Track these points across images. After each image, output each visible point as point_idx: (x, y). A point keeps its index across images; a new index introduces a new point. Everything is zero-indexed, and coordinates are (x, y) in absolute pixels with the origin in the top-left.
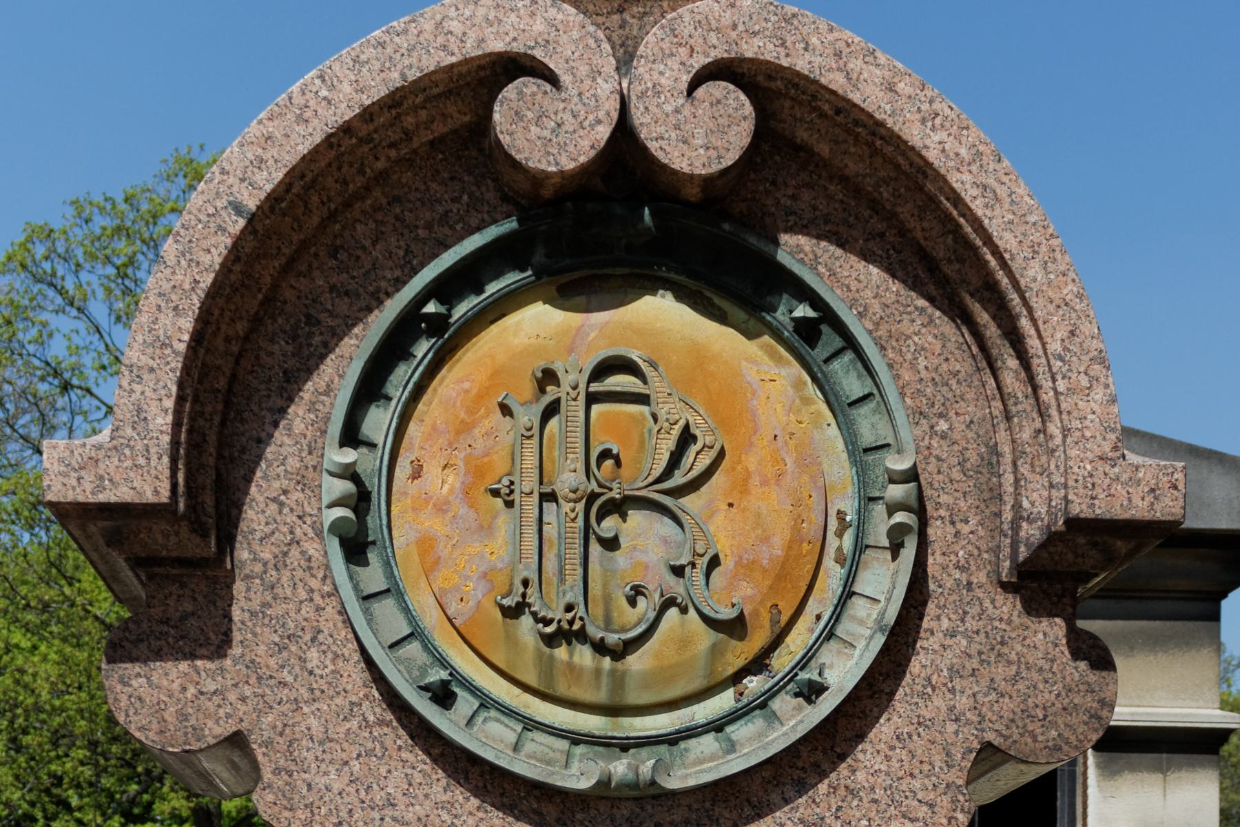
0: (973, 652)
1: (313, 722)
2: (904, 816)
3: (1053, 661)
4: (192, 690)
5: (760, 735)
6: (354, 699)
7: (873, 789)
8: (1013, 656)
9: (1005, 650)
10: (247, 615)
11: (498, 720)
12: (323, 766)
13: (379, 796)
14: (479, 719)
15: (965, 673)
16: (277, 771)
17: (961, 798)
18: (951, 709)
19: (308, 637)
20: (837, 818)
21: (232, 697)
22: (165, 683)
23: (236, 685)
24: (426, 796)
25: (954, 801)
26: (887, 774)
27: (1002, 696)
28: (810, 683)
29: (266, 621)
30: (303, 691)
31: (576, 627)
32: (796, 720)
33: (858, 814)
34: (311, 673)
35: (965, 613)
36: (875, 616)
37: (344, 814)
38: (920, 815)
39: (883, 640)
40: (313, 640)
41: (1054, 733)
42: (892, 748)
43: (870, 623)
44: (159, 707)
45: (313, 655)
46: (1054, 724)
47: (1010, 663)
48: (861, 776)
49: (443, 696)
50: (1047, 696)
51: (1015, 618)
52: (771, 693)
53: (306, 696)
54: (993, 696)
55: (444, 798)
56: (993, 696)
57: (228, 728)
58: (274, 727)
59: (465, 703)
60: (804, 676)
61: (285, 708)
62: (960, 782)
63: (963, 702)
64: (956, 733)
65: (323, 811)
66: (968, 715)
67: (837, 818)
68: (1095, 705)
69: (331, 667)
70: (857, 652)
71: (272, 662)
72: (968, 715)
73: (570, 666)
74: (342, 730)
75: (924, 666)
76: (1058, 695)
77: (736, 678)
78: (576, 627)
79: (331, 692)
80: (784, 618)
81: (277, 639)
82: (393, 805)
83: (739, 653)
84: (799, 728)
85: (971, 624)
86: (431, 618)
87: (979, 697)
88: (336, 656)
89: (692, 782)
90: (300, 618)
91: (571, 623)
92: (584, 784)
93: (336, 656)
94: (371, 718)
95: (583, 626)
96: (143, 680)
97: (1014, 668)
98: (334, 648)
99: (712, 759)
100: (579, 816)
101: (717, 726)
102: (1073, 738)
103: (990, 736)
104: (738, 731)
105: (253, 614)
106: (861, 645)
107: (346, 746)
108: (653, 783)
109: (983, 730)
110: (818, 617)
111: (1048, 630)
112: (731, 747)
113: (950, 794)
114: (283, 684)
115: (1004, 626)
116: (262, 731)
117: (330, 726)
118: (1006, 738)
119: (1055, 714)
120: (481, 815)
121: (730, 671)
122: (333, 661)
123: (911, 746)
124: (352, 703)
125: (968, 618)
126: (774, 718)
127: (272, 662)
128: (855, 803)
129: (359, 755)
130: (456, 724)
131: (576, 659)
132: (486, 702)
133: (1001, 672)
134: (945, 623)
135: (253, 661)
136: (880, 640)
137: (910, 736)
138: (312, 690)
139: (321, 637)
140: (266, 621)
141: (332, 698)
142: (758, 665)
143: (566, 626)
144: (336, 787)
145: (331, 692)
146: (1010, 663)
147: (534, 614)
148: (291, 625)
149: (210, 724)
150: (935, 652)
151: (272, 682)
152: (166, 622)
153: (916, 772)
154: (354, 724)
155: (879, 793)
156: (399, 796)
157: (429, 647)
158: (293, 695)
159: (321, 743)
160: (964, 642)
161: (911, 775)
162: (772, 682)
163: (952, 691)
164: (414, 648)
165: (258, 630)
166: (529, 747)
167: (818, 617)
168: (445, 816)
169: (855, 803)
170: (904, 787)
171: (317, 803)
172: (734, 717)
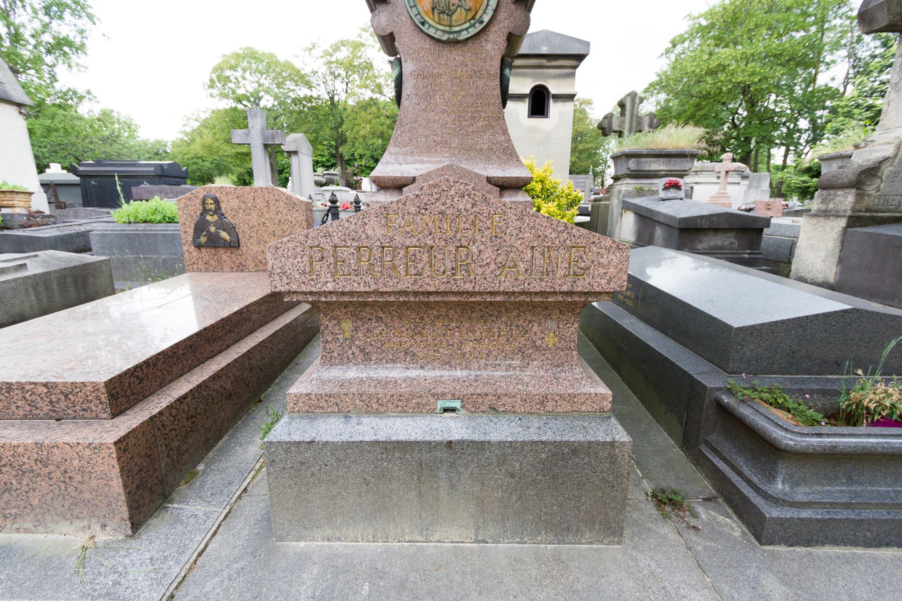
32: (479, 27)
49: (423, 24)
59: (427, 26)
83: (470, 16)
86: (421, 11)
101: (467, 29)
104: (470, 30)
132: (430, 26)
133: (512, 19)
142: (473, 18)
172: (469, 27)
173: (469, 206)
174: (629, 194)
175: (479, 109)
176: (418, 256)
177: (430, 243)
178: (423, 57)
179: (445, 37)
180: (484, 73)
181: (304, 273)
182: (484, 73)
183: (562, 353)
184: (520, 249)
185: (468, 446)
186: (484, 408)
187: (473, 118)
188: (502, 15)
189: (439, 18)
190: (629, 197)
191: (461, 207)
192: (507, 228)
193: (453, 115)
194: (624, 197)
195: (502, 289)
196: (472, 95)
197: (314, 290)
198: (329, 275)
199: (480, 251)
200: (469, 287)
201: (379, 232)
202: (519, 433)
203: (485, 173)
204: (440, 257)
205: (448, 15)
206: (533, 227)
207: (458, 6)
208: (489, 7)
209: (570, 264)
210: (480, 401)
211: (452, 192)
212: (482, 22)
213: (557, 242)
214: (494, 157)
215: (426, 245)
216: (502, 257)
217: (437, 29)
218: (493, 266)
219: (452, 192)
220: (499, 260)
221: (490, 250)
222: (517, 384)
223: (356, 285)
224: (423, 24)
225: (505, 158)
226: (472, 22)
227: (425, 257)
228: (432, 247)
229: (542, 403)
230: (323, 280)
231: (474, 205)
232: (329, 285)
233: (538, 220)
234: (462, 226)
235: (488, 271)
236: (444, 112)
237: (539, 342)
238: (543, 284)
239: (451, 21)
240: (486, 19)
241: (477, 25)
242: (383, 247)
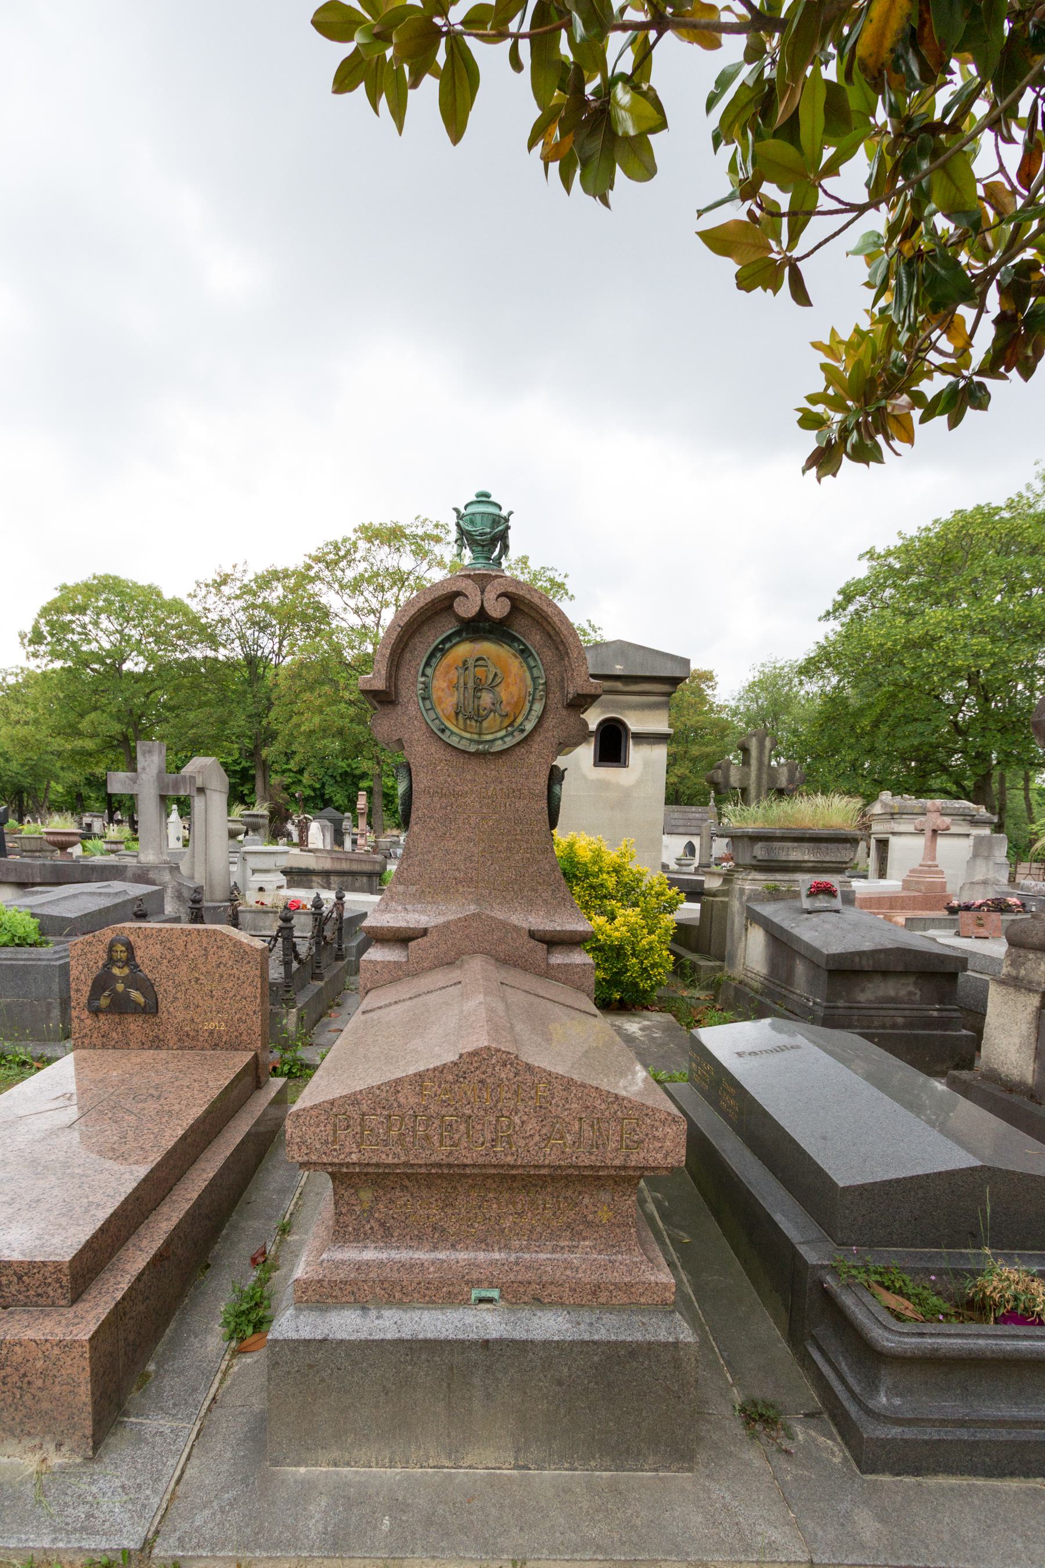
32: (519, 737)
49: (443, 731)
59: (448, 733)
83: (507, 722)
86: (441, 714)
101: (502, 738)
104: (507, 739)
112: (505, 743)
132: (452, 733)
133: (564, 727)
142: (511, 724)
164: (437, 721)
172: (505, 736)
173: (511, 1075)
174: (756, 896)
175: (518, 837)
176: (454, 1126)
177: (468, 1112)
178: (441, 770)
179: (472, 748)
180: (526, 792)
181: (327, 1142)
182: (526, 792)
183: (618, 1230)
184: (567, 1120)
185: (508, 1346)
186: (527, 1299)
187: (509, 849)
188: (550, 722)
189: (465, 723)
190: (756, 900)
191: (503, 1075)
192: (553, 1098)
193: (482, 845)
194: (748, 900)
195: (547, 1162)
196: (508, 819)
197: (336, 1161)
198: (354, 1145)
199: (523, 1122)
200: (510, 1160)
201: (412, 1100)
202: (567, 1330)
203: (525, 925)
204: (479, 1127)
205: (476, 721)
206: (581, 1098)
207: (491, 711)
208: (533, 713)
209: (622, 1137)
210: (522, 1290)
211: (493, 1061)
212: (523, 731)
213: (607, 1113)
214: (539, 901)
215: (463, 1114)
216: (547, 1128)
217: (462, 738)
218: (537, 1138)
219: (493, 1061)
220: (544, 1131)
221: (534, 1121)
222: (566, 1268)
223: (384, 1156)
224: (443, 731)
225: (555, 902)
226: (509, 729)
227: (462, 1127)
228: (470, 1117)
229: (594, 1293)
230: (347, 1150)
231: (516, 1074)
232: (353, 1156)
233: (586, 1091)
234: (504, 1095)
235: (532, 1143)
236: (469, 840)
237: (590, 1217)
238: (593, 1158)
239: (481, 728)
240: (529, 726)
242: (416, 1116)
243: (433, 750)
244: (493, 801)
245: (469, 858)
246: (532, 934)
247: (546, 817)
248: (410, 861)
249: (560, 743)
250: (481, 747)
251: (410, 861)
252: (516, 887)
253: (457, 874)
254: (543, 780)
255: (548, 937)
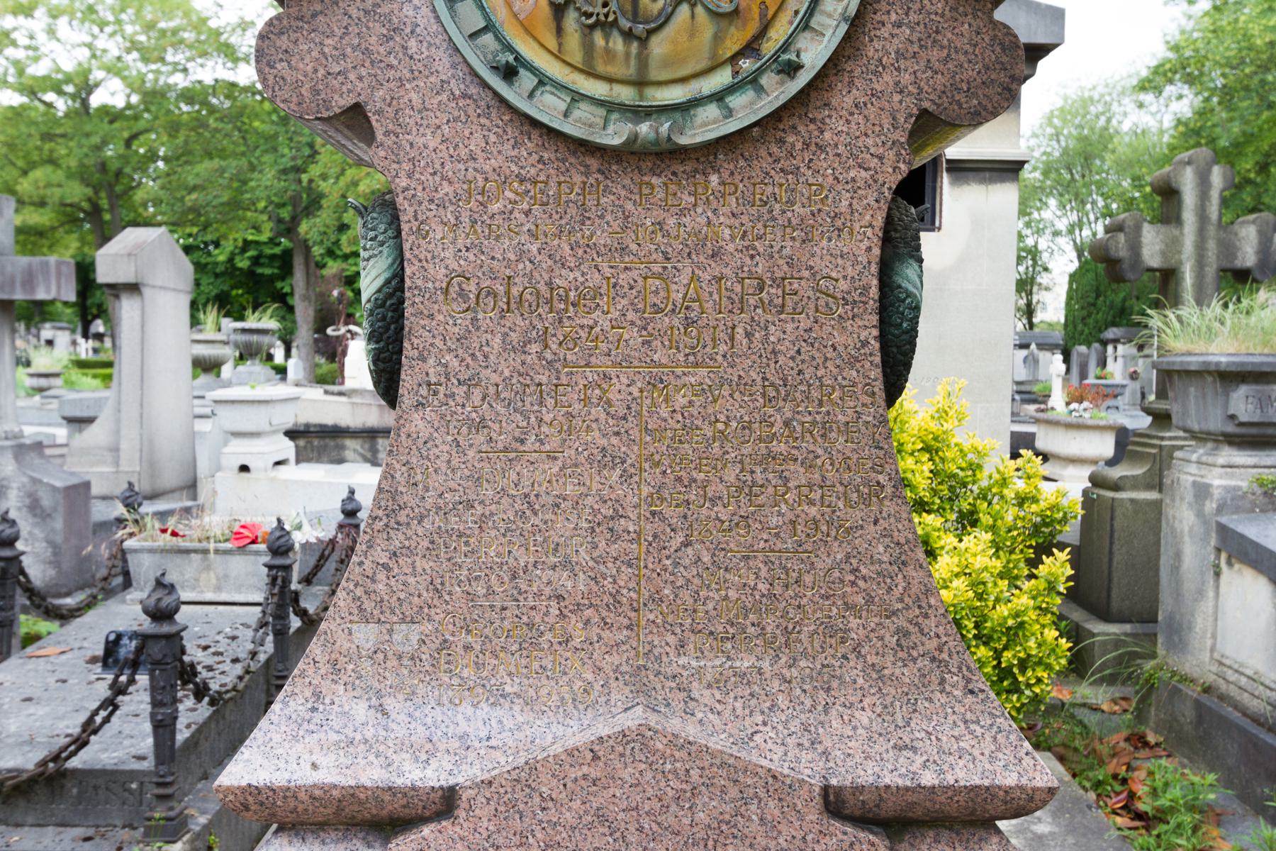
0: (915, 39)
1: (414, 96)
2: (860, 167)
3: (975, 46)
4: (321, 72)
5: (752, 103)
6: (444, 78)
7: (836, 145)
8: (945, 42)
9: (939, 37)
10: (362, 13)
11: (552, 93)
12: (421, 129)
13: (464, 153)
14: (538, 93)
15: (908, 55)
16: (387, 133)
17: (903, 152)
18: (897, 83)
19: (408, 30)
20: (809, 168)
21: (352, 76)
22: (301, 66)
23: (355, 67)
24: (499, 152)
25: (898, 154)
26: (848, 134)
27: (936, 73)
28: (789, 62)
29: (377, 17)
30: (405, 71)
31: (611, 19)
32: (778, 91)
33: (825, 165)
34: (411, 58)
35: (909, 8)
36: (840, 10)
37: (438, 166)
38: (872, 165)
39: (846, 27)
40: (412, 32)
41: (975, 102)
42: (852, 114)
43: (837, 16)
44: (298, 85)
45: (412, 43)
46: (976, 95)
47: (942, 47)
48: (827, 135)
49: (509, 73)
50: (970, 73)
51: (947, 12)
52: (760, 71)
53: (408, 75)
54: (929, 73)
55: (513, 154)
56: (929, 73)
57: (348, 101)
58: (384, 100)
59: (526, 80)
60: (785, 57)
61: (392, 85)
62: (903, 140)
63: (906, 78)
64: (901, 102)
65: (422, 163)
66: (910, 88)
67: (809, 168)
68: (1007, 80)
69: (426, 53)
70: (826, 39)
71: (382, 50)
72: (910, 88)
73: (607, 51)
74: (435, 102)
75: (877, 51)
76: (979, 73)
77: (734, 59)
78: (611, 19)
79: (427, 73)
80: (771, 13)
81: (385, 32)
82: (475, 159)
83: (735, 39)
84: (781, 97)
85: (913, 17)
86: (501, 16)
87: (919, 74)
88: (430, 44)
89: (699, 139)
90: (402, 15)
91: (606, 16)
92: (616, 141)
93: (430, 44)
94: (457, 93)
95: (616, 19)
96: (285, 64)
97: (946, 51)
98: (428, 38)
99: (714, 122)
100: (614, 167)
101: (719, 97)
102: (989, 106)
103: (926, 105)
104: (735, 101)
105: (366, 12)
106: (829, 33)
107: (438, 114)
108: (669, 139)
109: (921, 100)
110: (796, 12)
111: (972, 21)
112: (729, 113)
113: (895, 149)
114: (390, 66)
115: (938, 19)
116: (375, 102)
117: (426, 99)
118: (938, 106)
119: (976, 87)
120: (540, 166)
121: (729, 54)
122: (428, 48)
123: (866, 112)
124: (442, 81)
125: (911, 13)
126: (760, 90)
127: (382, 50)
128: (823, 156)
129: (448, 121)
130: (519, 95)
131: (611, 44)
132: (543, 81)
133: (935, 54)
134: (894, 17)
135: (367, 49)
136: (844, 28)
137: (865, 104)
138: (412, 71)
139: (418, 30)
140: (377, 17)
141: (427, 77)
142: (751, 48)
143: (602, 18)
144: (432, 145)
145: (427, 73)
146: (942, 47)
147: (578, 9)
148: (396, 21)
149: (336, 97)
150: (885, 39)
151: (382, 65)
152: (301, 19)
153: (870, 132)
154: (444, 97)
155: (841, 149)
156: (479, 152)
157: (499, 38)
158: (398, 75)
159: (420, 112)
160: (908, 32)
161: (866, 135)
162: (759, 64)
163: (898, 69)
164: (488, 38)
165: (371, 25)
166: (576, 114)
167: (796, 12)
168: (514, 168)
169: (823, 156)
170: (860, 144)
171: (418, 158)
172: (731, 89)
174: (1234, 502)
175: (780, 447)
178: (507, 214)
179: (615, 134)
187: (748, 489)
188: (887, 39)
189: (588, 48)
190: (1237, 510)
193: (652, 476)
194: (1220, 510)
196: (742, 385)
205: (628, 35)
212: (792, 69)
214: (853, 671)
217: (578, 97)
224: (509, 73)
225: (908, 674)
226: (746, 65)
236: (606, 459)
239: (643, 62)
240: (814, 54)
241: (767, 80)
243: (476, 144)
244: (689, 323)
245: (606, 524)
246: (835, 804)
247: (876, 373)
248: (398, 540)
249: (924, 113)
250: (644, 128)
251: (398, 540)
252: (770, 623)
253: (564, 580)
254: (864, 245)
255: (889, 809)
